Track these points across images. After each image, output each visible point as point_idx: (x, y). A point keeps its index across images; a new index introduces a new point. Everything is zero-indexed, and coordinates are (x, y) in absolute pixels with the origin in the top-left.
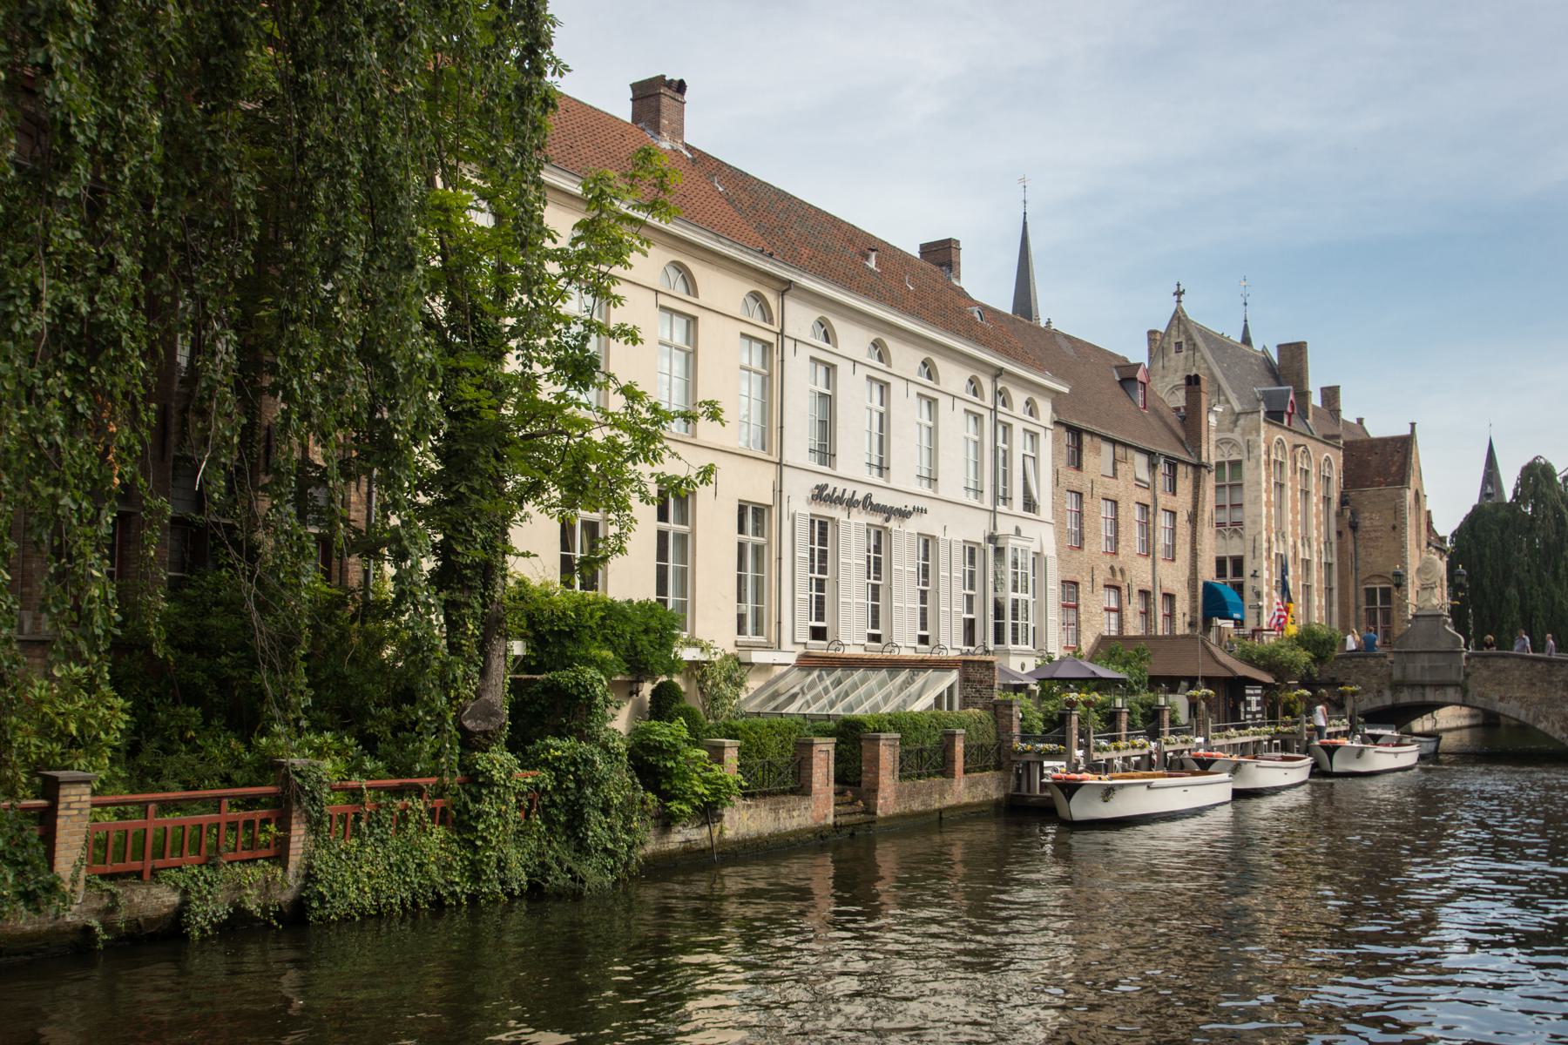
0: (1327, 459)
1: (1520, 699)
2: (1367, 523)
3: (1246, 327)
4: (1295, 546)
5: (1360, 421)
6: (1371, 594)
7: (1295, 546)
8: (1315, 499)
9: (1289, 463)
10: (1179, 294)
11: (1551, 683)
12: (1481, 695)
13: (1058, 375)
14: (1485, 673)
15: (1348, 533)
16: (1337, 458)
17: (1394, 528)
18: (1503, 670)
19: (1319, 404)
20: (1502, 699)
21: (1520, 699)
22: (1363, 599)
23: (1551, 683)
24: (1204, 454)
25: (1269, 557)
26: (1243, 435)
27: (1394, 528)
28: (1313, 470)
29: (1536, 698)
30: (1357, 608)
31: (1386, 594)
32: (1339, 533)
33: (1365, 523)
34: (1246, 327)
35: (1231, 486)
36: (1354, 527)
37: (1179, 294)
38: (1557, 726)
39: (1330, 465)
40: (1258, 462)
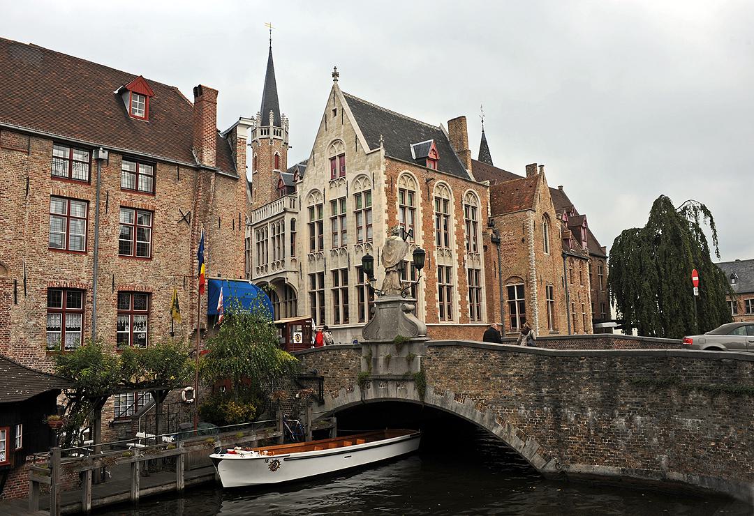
1: (474, 397)
2: (506, 239)
3: (483, 135)
5: (561, 187)
6: (511, 289)
10: (335, 75)
11: (505, 377)
12: (437, 392)
15: (492, 248)
17: (523, 240)
18: (456, 362)
19: (476, 158)
20: (457, 397)
21: (474, 397)
22: (506, 295)
26: (370, 170)
27: (523, 240)
28: (452, 200)
29: (490, 396)
30: (502, 302)
31: (521, 288)
32: (485, 247)
33: (504, 239)
34: (483, 135)
36: (496, 242)
37: (335, 75)
38: (514, 431)
40: (380, 190)
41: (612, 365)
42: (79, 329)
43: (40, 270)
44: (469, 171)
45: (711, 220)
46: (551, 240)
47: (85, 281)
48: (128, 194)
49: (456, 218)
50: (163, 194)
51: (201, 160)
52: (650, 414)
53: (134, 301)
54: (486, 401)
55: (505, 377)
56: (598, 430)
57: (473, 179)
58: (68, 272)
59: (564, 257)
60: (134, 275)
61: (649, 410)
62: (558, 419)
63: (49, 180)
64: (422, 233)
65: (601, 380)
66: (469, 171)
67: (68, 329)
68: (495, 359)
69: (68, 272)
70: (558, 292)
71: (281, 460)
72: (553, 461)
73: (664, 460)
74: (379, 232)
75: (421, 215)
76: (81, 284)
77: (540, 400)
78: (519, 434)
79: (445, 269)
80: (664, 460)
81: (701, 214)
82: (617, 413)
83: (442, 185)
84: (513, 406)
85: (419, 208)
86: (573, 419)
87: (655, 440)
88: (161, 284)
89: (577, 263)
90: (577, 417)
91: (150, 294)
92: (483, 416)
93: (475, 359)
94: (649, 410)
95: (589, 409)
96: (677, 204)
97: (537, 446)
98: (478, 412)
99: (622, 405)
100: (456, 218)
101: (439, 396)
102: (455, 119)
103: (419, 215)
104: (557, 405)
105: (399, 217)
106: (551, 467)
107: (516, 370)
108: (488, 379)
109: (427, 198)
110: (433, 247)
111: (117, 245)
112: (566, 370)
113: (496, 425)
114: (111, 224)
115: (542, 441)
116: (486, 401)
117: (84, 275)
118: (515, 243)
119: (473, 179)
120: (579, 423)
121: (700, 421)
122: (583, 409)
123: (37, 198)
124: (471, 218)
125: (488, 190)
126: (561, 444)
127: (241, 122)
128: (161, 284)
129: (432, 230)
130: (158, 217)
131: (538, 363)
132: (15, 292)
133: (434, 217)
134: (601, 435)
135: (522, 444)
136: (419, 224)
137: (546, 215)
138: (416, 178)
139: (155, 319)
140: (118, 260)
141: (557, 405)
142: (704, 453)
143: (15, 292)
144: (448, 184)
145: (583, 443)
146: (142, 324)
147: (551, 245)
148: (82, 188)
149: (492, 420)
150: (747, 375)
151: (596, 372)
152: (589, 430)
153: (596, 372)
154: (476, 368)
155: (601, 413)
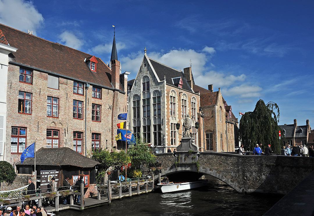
0: (194, 98)
11: (227, 164)
12: (204, 168)
13: (12, 45)
16: (198, 98)
20: (210, 170)
25: (168, 124)
28: (187, 100)
29: (222, 169)
30: (204, 139)
38: (229, 180)
40: (164, 97)
41: (261, 160)
42: (80, 146)
43: (71, 125)
44: (192, 89)
45: (278, 109)
46: (222, 116)
47: (83, 129)
48: (94, 99)
49: (189, 107)
50: (104, 99)
51: (115, 87)
53: (96, 136)
54: (220, 171)
55: (227, 164)
56: (257, 179)
57: (193, 92)
58: (78, 126)
59: (226, 123)
60: (96, 127)
61: (272, 173)
62: (244, 175)
63: (73, 94)
64: (178, 113)
65: (258, 164)
66: (192, 89)
67: (78, 146)
69: (78, 126)
70: (224, 136)
71: (290, 155)
72: (242, 189)
73: (276, 187)
74: (164, 112)
75: (177, 106)
76: (82, 130)
77: (238, 171)
78: (231, 181)
79: (173, 124)
80: (276, 187)
81: (274, 107)
83: (184, 94)
85: (177, 104)
87: (274, 181)
88: (103, 131)
89: (230, 124)
90: (250, 175)
91: (100, 134)
94: (272, 173)
96: (266, 103)
97: (237, 184)
99: (264, 172)
100: (189, 107)
101: (204, 170)
102: (187, 68)
103: (177, 106)
104: (244, 172)
105: (170, 107)
106: (241, 191)
107: (231, 161)
108: (221, 164)
109: (179, 100)
110: (181, 118)
111: (91, 117)
112: (247, 161)
113: (224, 178)
114: (90, 109)
115: (239, 183)
116: (220, 171)
117: (83, 127)
119: (193, 92)
122: (252, 173)
123: (70, 101)
124: (193, 107)
125: (199, 96)
126: (245, 183)
127: (126, 73)
128: (103, 131)
129: (181, 112)
130: (103, 107)
131: (238, 159)
132: (65, 133)
133: (182, 106)
134: (257, 180)
135: (232, 184)
136: (177, 109)
137: (221, 107)
138: (176, 92)
139: (102, 143)
140: (92, 122)
141: (244, 172)
143: (65, 133)
144: (186, 94)
145: (252, 183)
146: (98, 145)
147: (222, 118)
148: (82, 97)
149: (222, 176)
150: (301, 163)
151: (256, 162)
153: (256, 162)
155: (258, 174)
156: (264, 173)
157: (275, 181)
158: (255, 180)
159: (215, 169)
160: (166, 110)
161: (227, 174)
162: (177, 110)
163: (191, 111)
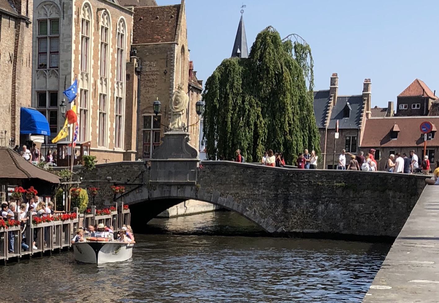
0: (122, 20)
4: (95, 84)
7: (95, 84)
8: (111, 50)
9: (93, 22)
14: (213, 176)
16: (130, 21)
20: (222, 195)
23: (255, 183)
24: (23, 10)
28: (111, 29)
35: (50, 38)
39: (124, 26)
52: (338, 203)
68: (250, 173)
82: (320, 202)
84: (259, 200)
85: (92, 38)
86: (295, 206)
87: (339, 215)
90: (297, 206)
92: (238, 206)
93: (237, 173)
95: (305, 201)
98: (236, 203)
100: (112, 47)
107: (263, 179)
115: (275, 218)
118: (157, 74)
120: (298, 208)
121: (363, 205)
122: (301, 200)
133: (100, 45)
134: (309, 214)
142: (363, 220)
152: (303, 211)
154: (237, 178)
156: (322, 201)
157: (341, 215)
158: (305, 213)
159: (231, 194)
160: (73, 56)
161: (254, 203)
162: (92, 54)
163: (116, 55)
